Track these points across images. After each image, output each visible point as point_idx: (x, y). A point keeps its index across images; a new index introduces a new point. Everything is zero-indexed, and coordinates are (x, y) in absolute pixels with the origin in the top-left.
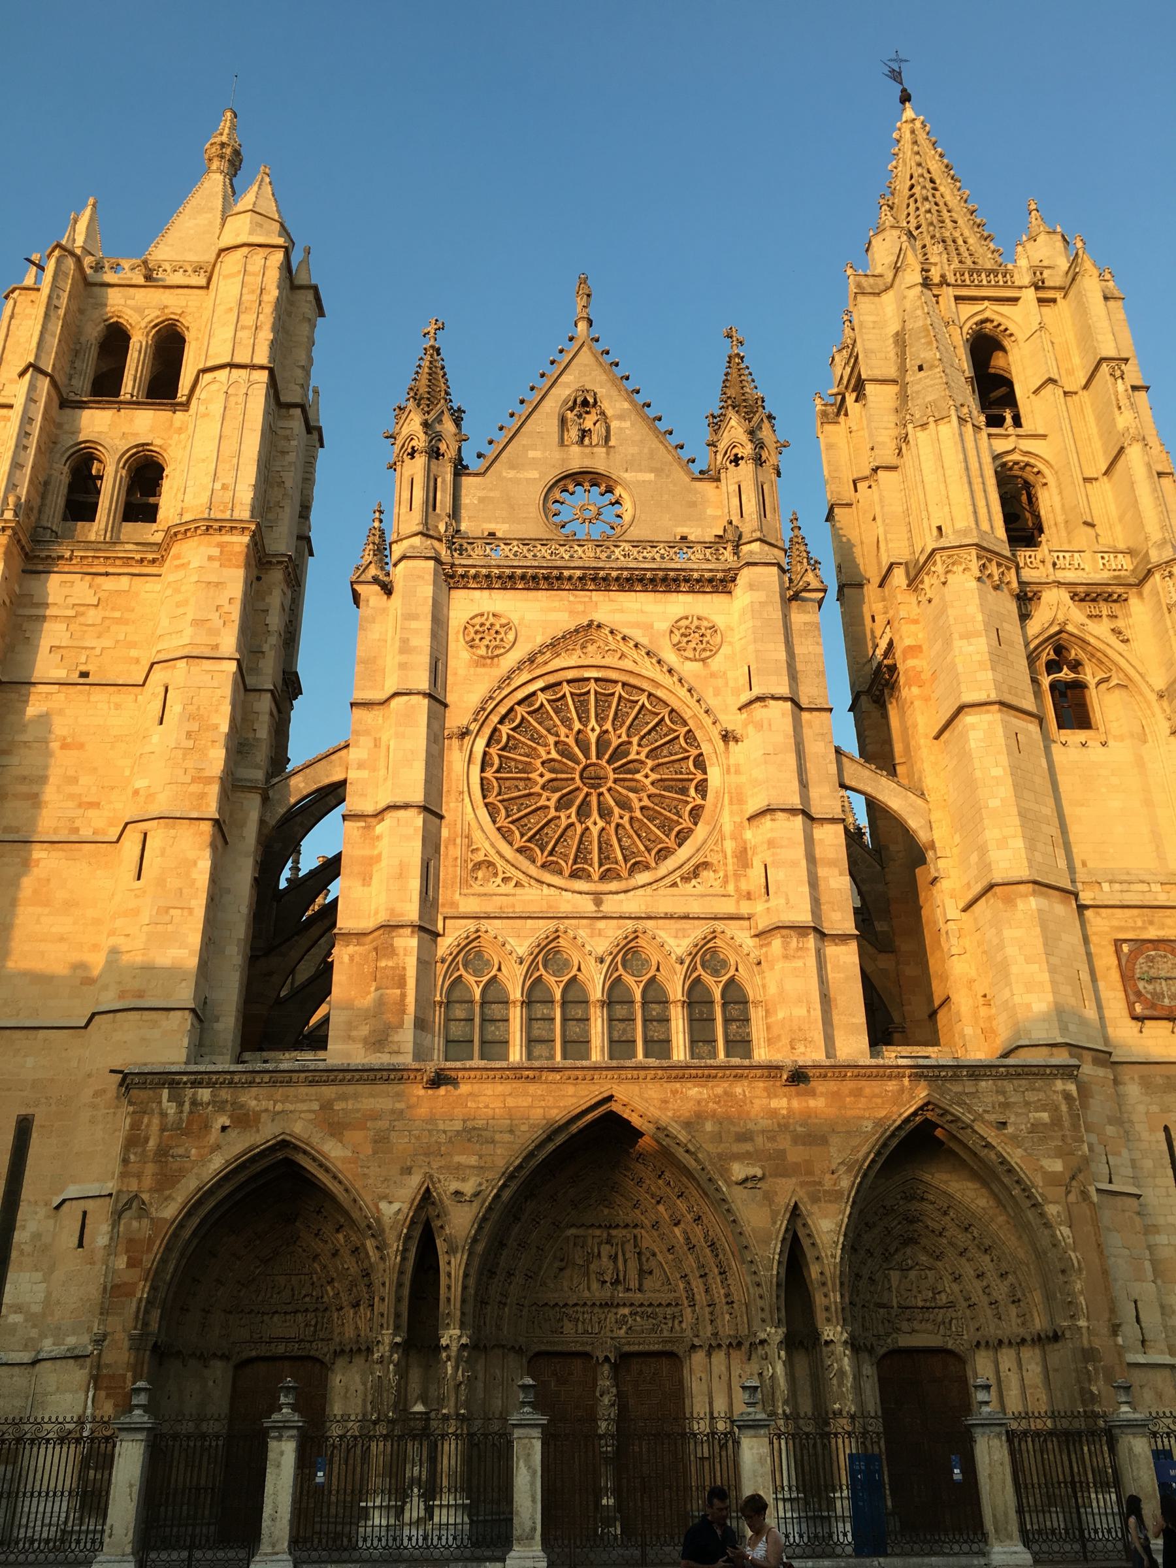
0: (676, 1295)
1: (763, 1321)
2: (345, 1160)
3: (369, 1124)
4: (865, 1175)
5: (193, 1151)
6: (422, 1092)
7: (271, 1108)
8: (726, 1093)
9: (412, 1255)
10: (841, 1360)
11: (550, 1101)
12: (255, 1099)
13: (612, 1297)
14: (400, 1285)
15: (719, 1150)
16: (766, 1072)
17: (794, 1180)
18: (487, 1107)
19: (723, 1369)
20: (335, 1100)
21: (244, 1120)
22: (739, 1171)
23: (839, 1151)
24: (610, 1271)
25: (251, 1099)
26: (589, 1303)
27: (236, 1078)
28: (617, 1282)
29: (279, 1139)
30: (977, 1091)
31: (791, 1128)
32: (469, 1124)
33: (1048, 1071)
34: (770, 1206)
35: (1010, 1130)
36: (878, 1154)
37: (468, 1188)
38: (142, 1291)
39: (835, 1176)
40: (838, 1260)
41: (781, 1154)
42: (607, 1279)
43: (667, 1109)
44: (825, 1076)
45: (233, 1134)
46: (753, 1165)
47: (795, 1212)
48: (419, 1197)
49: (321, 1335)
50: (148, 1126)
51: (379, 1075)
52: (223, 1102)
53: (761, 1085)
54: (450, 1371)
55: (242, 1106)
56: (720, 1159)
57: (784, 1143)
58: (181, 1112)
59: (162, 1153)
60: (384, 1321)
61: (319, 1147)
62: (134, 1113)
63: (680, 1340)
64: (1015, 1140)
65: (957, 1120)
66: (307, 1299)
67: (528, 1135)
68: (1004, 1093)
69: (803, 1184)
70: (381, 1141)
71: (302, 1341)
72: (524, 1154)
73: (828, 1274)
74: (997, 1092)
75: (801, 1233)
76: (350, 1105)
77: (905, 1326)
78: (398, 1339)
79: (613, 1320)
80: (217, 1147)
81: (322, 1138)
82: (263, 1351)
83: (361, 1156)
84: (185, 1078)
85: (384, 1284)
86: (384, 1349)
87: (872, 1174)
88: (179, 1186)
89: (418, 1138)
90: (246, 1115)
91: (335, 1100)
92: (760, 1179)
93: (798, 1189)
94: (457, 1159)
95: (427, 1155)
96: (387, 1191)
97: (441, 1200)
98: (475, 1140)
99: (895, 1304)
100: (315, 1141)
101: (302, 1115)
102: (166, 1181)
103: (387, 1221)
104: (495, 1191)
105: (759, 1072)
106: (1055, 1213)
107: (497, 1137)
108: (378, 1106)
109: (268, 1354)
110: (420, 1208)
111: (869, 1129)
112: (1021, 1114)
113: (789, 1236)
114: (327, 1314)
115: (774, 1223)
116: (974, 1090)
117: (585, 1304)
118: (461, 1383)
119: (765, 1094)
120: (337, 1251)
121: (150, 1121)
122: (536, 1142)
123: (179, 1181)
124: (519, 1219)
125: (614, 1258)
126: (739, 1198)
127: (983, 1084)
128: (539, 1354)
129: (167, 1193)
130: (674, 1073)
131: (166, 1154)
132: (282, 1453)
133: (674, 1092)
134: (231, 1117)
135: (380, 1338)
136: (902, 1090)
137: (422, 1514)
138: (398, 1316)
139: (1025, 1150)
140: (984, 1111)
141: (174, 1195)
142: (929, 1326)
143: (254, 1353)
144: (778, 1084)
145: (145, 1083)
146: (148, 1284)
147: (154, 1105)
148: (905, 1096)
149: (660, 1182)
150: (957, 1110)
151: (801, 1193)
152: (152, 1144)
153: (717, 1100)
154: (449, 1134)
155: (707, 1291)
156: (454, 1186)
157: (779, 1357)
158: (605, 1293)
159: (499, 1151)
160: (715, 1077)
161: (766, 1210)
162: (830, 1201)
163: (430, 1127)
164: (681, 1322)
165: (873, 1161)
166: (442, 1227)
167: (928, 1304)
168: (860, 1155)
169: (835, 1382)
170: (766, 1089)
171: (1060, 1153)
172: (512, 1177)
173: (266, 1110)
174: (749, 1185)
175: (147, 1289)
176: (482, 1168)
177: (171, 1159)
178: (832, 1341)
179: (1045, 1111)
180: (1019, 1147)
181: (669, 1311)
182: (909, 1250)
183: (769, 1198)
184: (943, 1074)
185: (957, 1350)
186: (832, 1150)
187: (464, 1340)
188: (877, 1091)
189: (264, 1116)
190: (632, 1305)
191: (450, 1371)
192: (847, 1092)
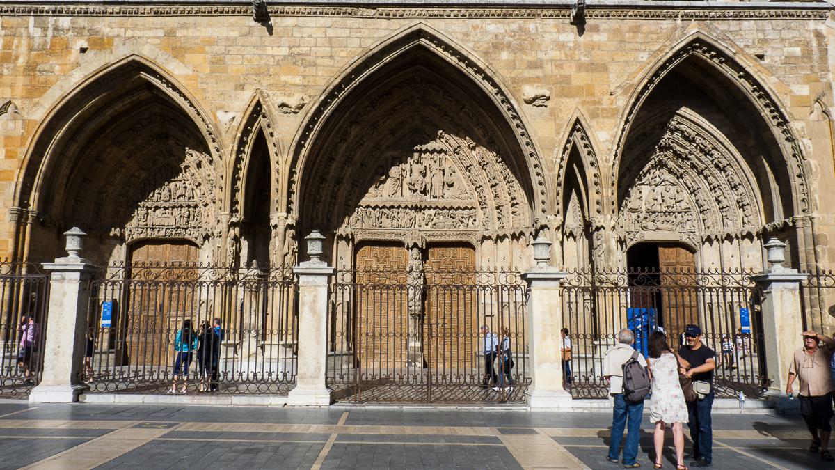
0: (472, 201)
1: (544, 211)
2: (186, 77)
3: (207, 48)
4: (638, 99)
5: (57, 68)
6: (253, 23)
7: (122, 34)
8: (520, 28)
9: (246, 156)
10: (609, 241)
11: (366, 33)
12: (109, 26)
13: (421, 201)
14: (235, 180)
15: (513, 76)
16: (557, 11)
17: (577, 100)
18: (310, 36)
19: (507, 252)
20: (177, 28)
21: (99, 43)
22: (530, 91)
23: (618, 77)
24: (420, 182)
25: (106, 26)
26: (403, 206)
27: (91, 8)
28: (424, 192)
29: (130, 59)
30: (740, 29)
31: (577, 58)
32: (295, 50)
33: (804, 12)
34: (555, 120)
35: (767, 61)
36: (651, 81)
37: (293, 102)
38: (19, 176)
39: (613, 97)
40: (611, 164)
41: (567, 79)
42: (417, 187)
43: (469, 41)
44: (608, 16)
45: (90, 54)
46: (542, 88)
47: (577, 126)
48: (251, 109)
49: (193, 224)
50: (17, 47)
51: (215, 8)
52: (81, 28)
53: (552, 22)
54: (277, 243)
55: (97, 32)
56: (514, 82)
57: (570, 70)
58: (46, 36)
59: (30, 69)
60: (222, 205)
61: (164, 66)
62: (5, 35)
63: (473, 232)
64: (771, 70)
65: (720, 54)
66: (182, 199)
67: (346, 60)
68: (763, 31)
69: (584, 103)
70: (218, 62)
71: (178, 228)
72: (343, 76)
73: (602, 175)
74: (758, 30)
75: (580, 144)
76: (190, 33)
77: (650, 225)
78: (234, 219)
79: (421, 219)
80: (78, 65)
81: (167, 60)
82: (149, 234)
83: (201, 75)
84: (47, 7)
85: (222, 177)
86: (223, 226)
87: (643, 98)
88: (45, 95)
89: (250, 61)
90: (102, 39)
91: (177, 28)
92: (548, 99)
93: (580, 107)
94: (283, 78)
95: (257, 74)
96: (224, 103)
97: (270, 111)
98: (300, 63)
99: (644, 210)
100: (160, 61)
101: (149, 40)
102: (35, 91)
103: (223, 129)
104: (317, 105)
105: (551, 11)
106: (800, 129)
107: (319, 61)
108: (215, 34)
109: (153, 236)
110: (252, 119)
111: (644, 59)
112: (777, 48)
113: (569, 146)
114: (197, 209)
115: (559, 133)
116: (737, 29)
117: (399, 207)
118: (288, 253)
119: (556, 30)
120: (200, 162)
121: (19, 42)
122: (354, 66)
123: (45, 91)
124: (345, 140)
125: (424, 175)
126: (526, 112)
127: (746, 24)
128: (364, 243)
129: (36, 100)
130: (476, 10)
131: (34, 69)
132: (64, 294)
133: (475, 28)
134: (88, 40)
135: (219, 219)
136: (675, 28)
137: (253, 350)
138: (234, 203)
139: (778, 78)
140: (748, 46)
141: (42, 102)
142: (669, 226)
143: (142, 236)
144: (567, 21)
145: (13, 11)
146: (23, 172)
147: (23, 30)
148: (678, 33)
149: (462, 114)
150: (721, 45)
151: (583, 110)
152: (21, 61)
153: (513, 34)
154: (277, 58)
155: (497, 196)
156: (282, 100)
157: (557, 239)
158: (416, 198)
159: (320, 73)
160: (511, 15)
161: (551, 124)
162: (607, 117)
163: (260, 52)
164: (475, 220)
165: (646, 87)
166: (272, 135)
167: (670, 209)
168: (636, 81)
169: (603, 257)
170: (556, 26)
171: (807, 80)
172: (331, 96)
173: (118, 36)
174: (538, 102)
175: (22, 175)
176: (305, 86)
177: (38, 73)
178: (602, 227)
179: (798, 45)
180: (773, 75)
181: (467, 212)
182: (657, 173)
183: (554, 115)
184: (712, 14)
185: (690, 242)
186: (612, 76)
187: (290, 221)
188: (653, 28)
189: (116, 41)
190: (437, 207)
191: (277, 243)
192: (627, 29)
